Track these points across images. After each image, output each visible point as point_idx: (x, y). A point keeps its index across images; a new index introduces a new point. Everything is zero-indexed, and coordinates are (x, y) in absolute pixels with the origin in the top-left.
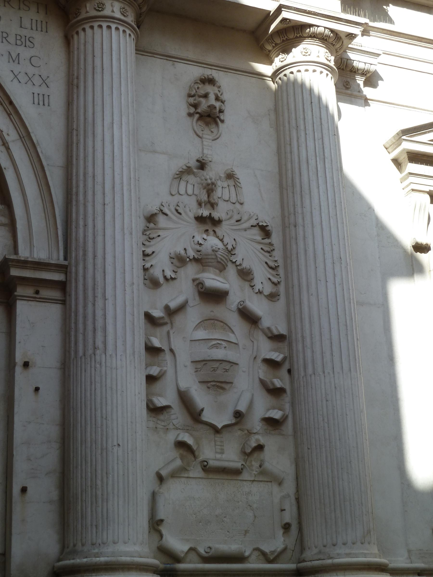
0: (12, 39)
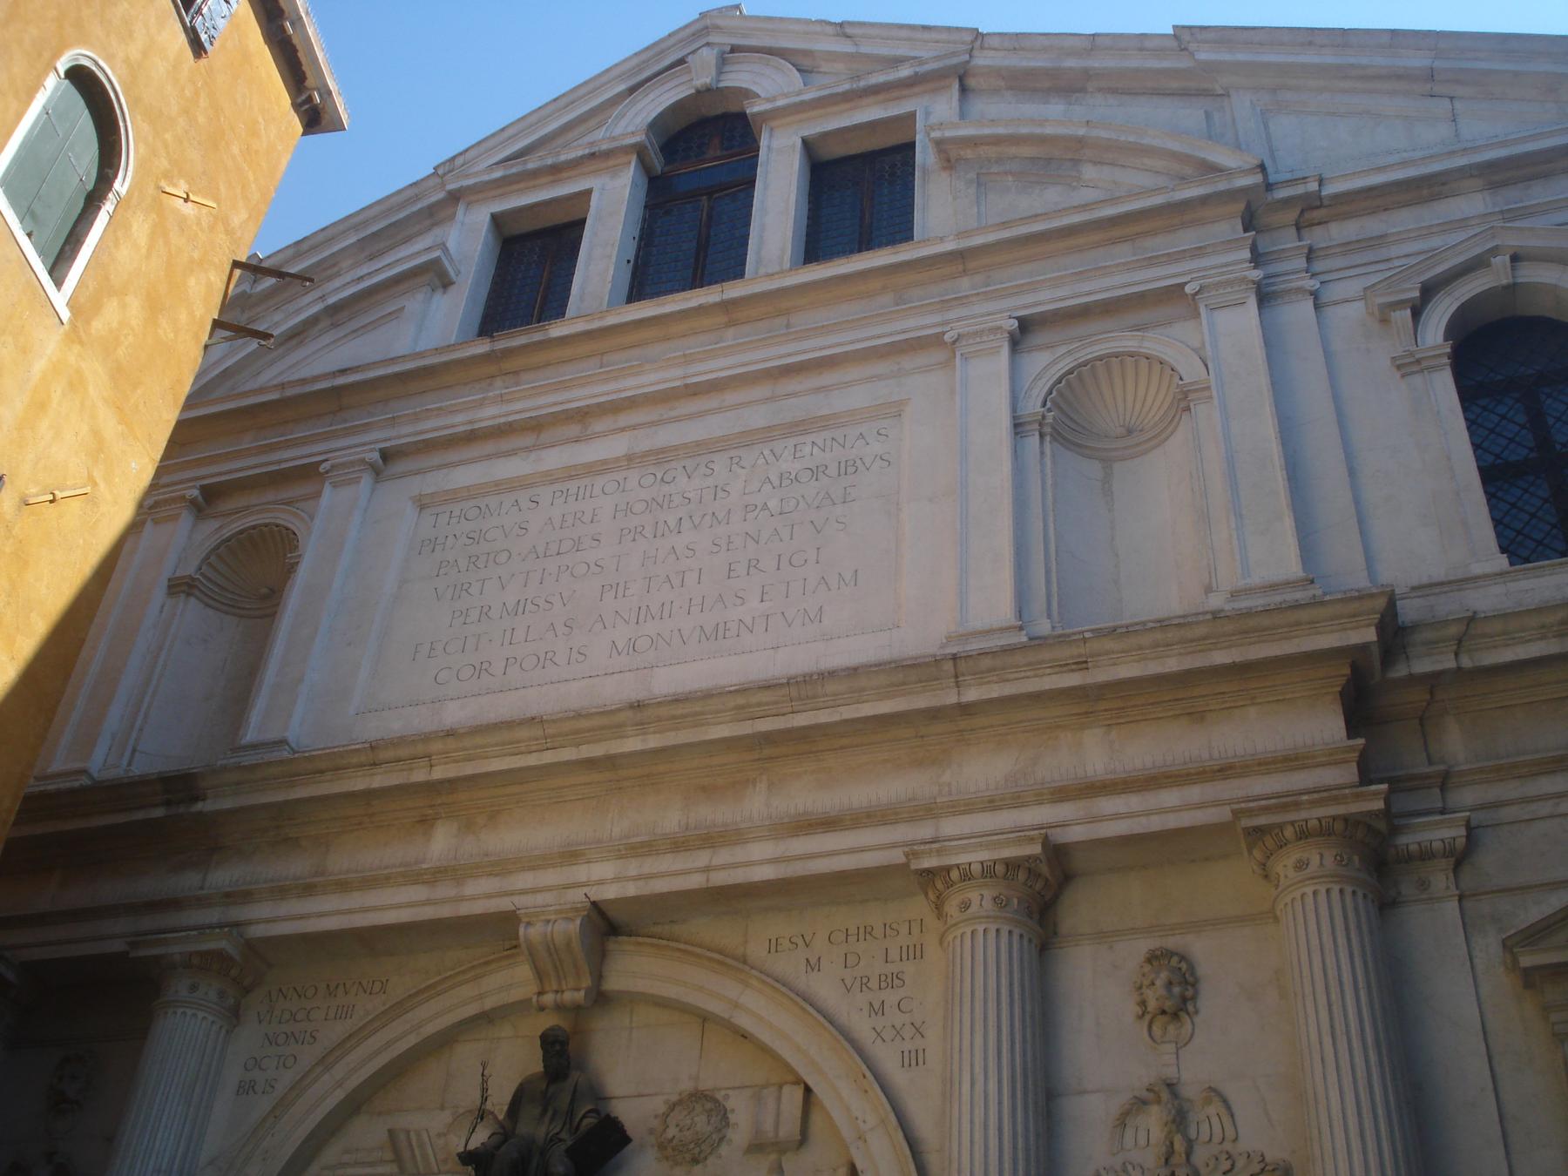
0: (874, 984)
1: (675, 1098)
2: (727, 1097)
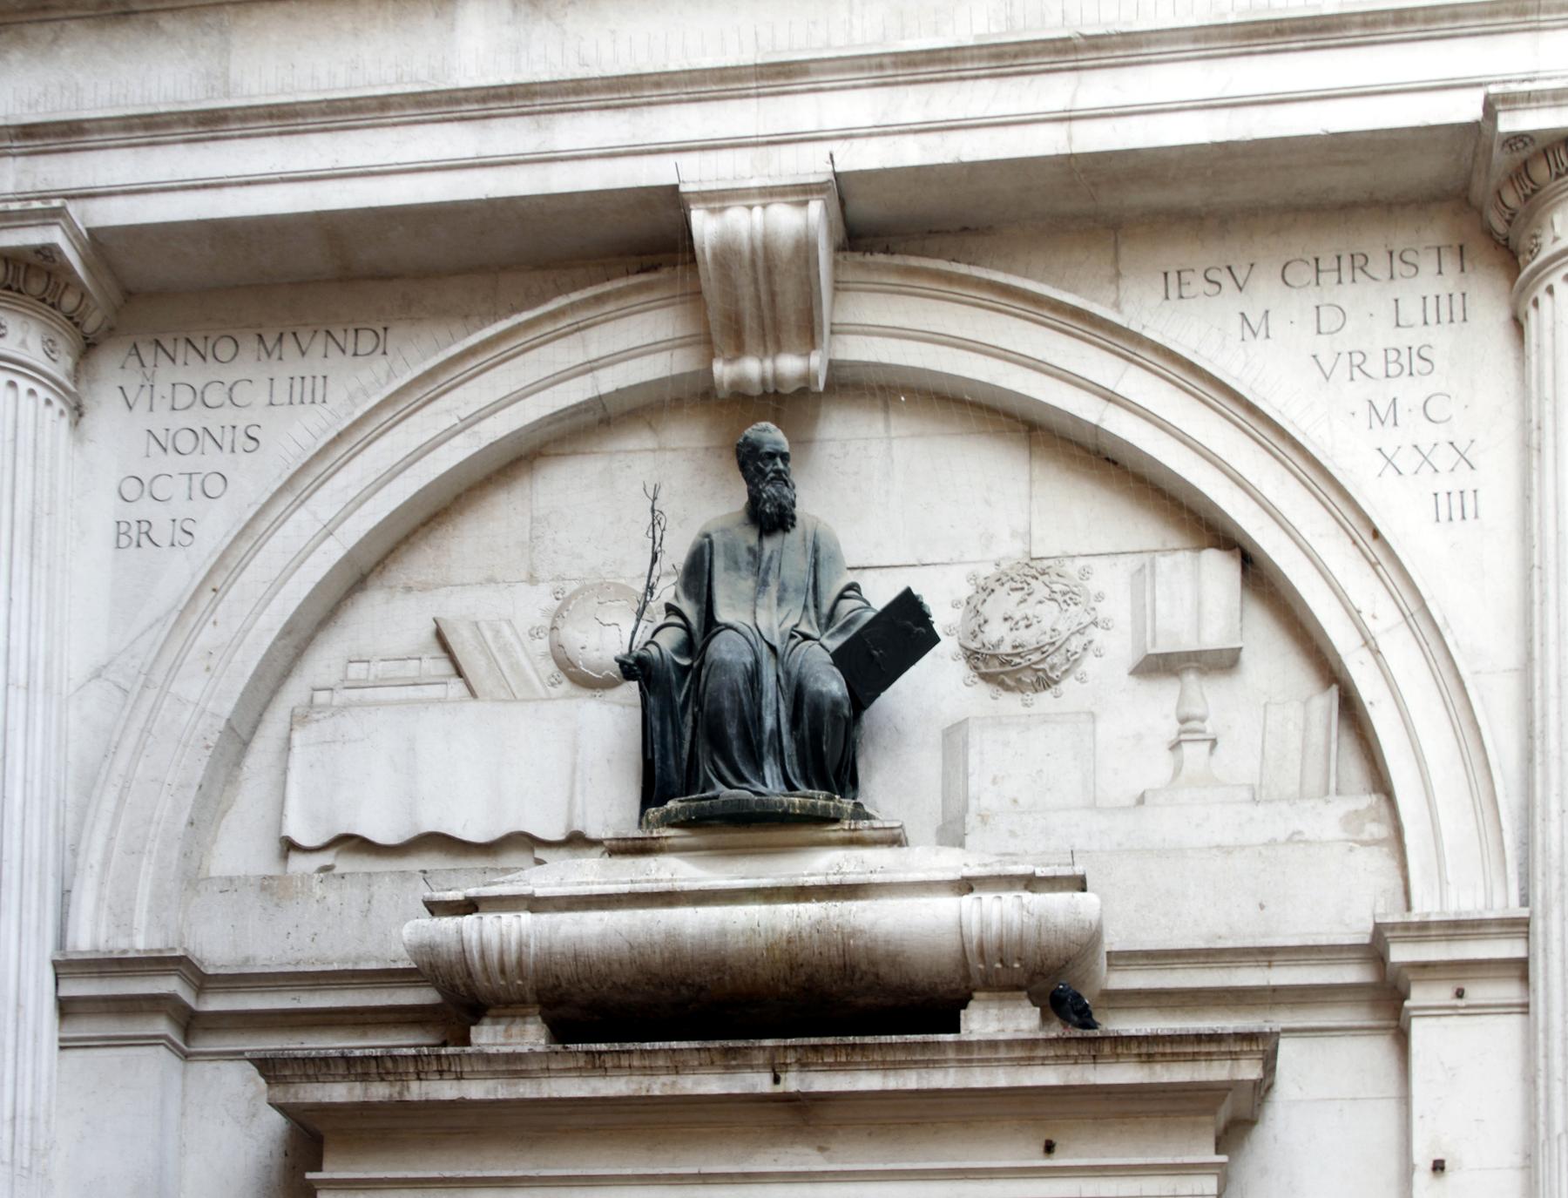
1: (989, 570)
2: (1085, 574)
